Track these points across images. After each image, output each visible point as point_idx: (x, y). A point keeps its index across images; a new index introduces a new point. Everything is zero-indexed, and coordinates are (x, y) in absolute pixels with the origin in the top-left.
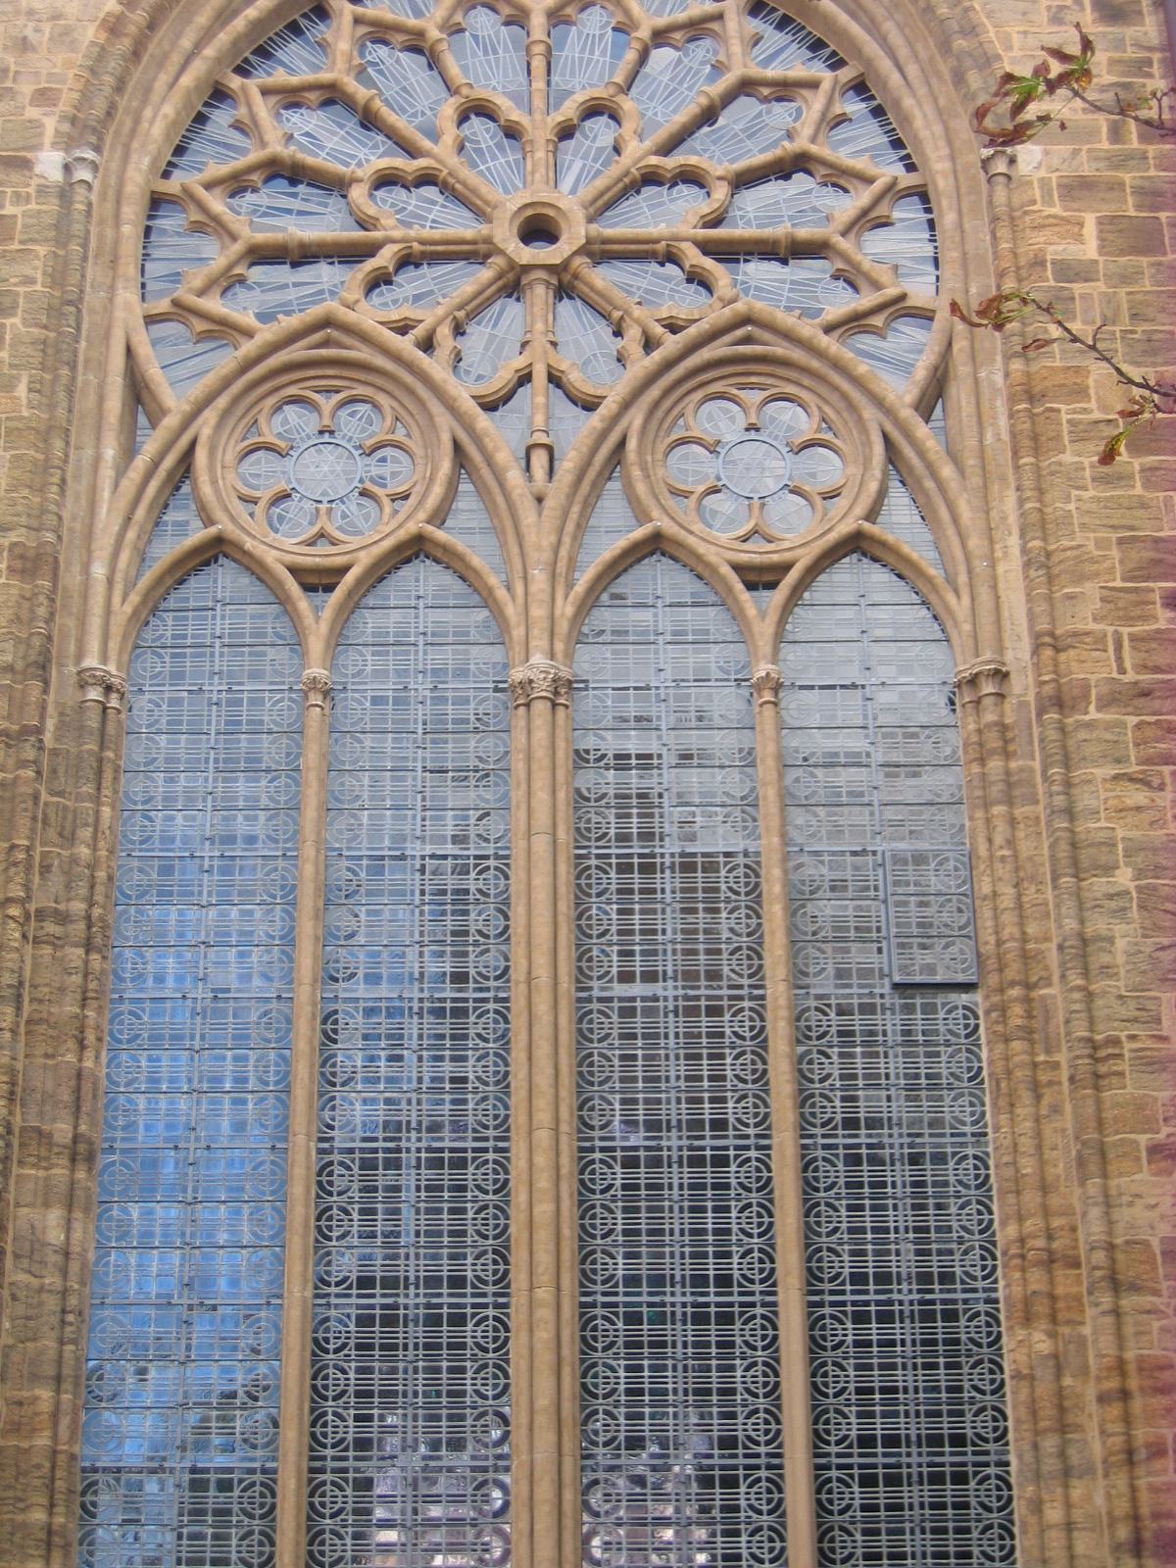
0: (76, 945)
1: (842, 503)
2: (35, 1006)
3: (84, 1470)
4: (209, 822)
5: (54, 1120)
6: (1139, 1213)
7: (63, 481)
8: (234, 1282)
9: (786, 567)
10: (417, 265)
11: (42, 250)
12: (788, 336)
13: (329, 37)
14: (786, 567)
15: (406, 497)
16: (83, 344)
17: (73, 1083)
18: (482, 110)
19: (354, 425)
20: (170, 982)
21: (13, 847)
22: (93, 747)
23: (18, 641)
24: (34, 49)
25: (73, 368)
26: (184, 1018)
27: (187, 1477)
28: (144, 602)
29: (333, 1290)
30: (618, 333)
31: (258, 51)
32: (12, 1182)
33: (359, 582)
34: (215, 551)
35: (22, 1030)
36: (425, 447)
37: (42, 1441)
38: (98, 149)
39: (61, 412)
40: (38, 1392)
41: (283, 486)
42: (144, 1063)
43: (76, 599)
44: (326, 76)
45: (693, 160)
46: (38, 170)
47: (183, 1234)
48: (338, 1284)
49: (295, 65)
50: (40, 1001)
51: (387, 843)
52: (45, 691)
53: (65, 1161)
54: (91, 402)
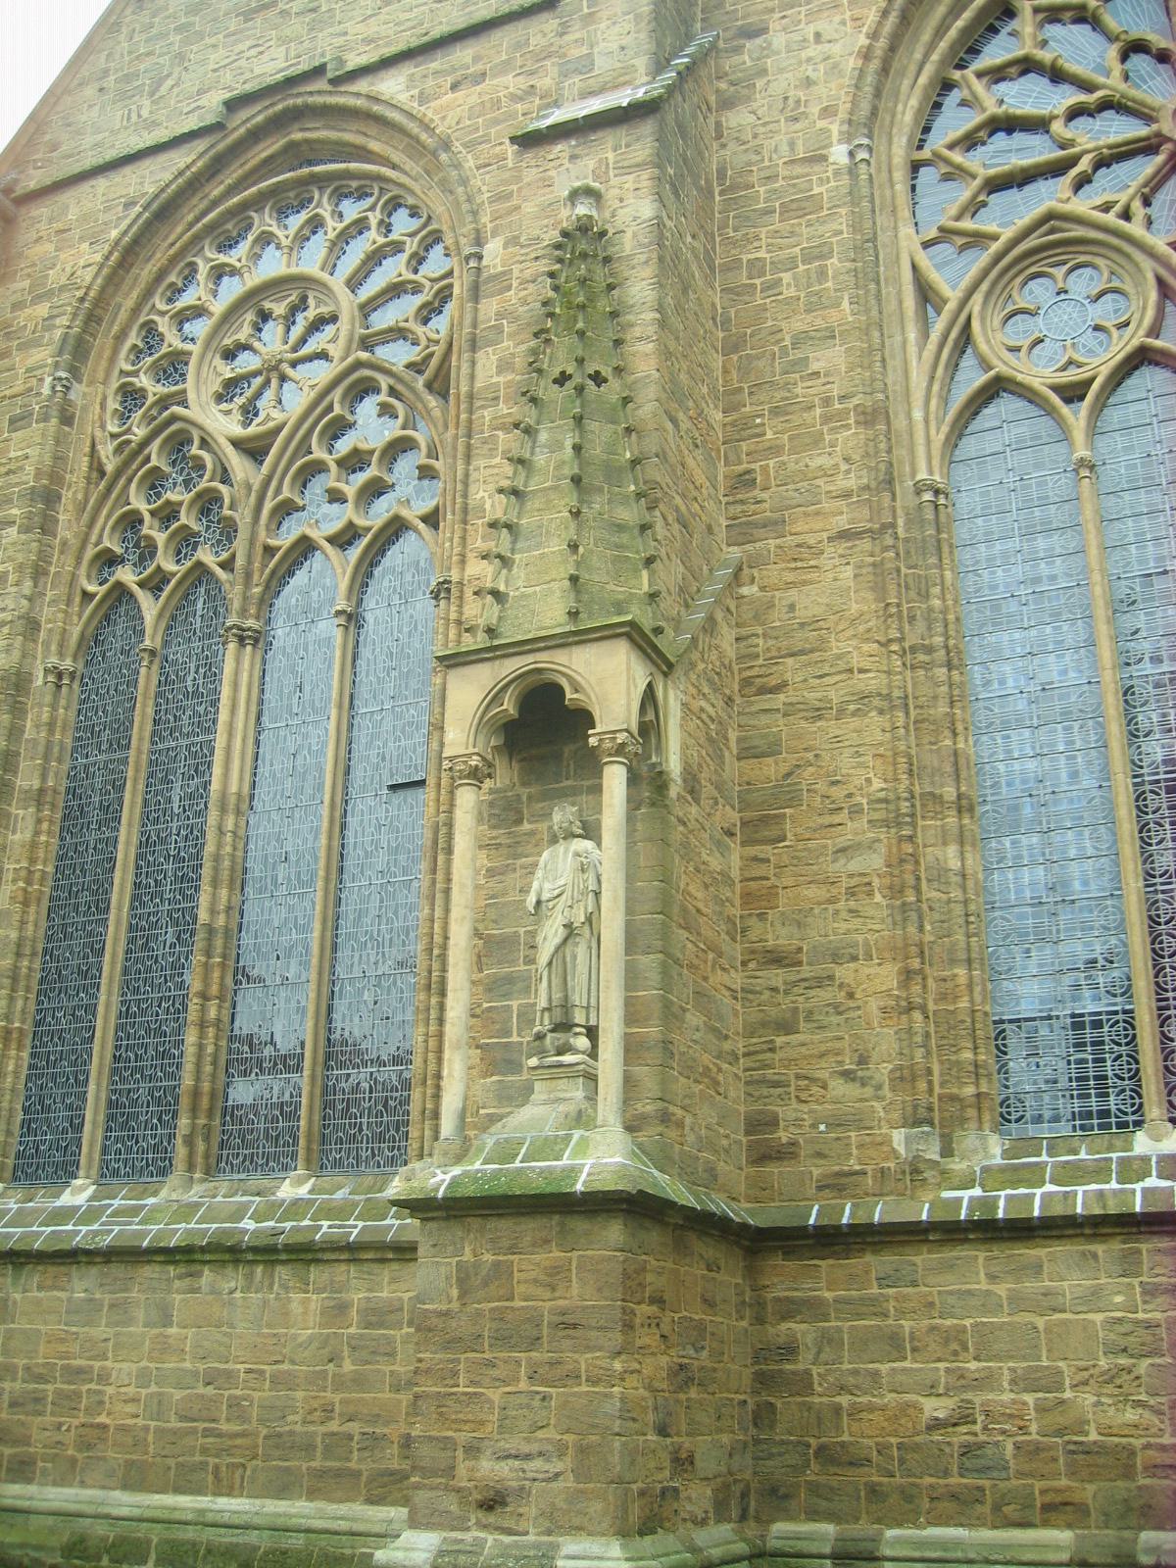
0: (941, 666)
2: (918, 711)
3: (995, 1022)
4: (1019, 571)
5: (942, 786)
7: (883, 360)
8: (1085, 883)
10: (1108, 166)
11: (843, 211)
15: (1128, 324)
16: (882, 269)
17: (952, 759)
19: (1082, 284)
20: (1010, 683)
21: (888, 605)
22: (931, 532)
23: (870, 468)
24: (815, 83)
25: (878, 283)
26: (1021, 705)
27: (1069, 1021)
28: (951, 431)
29: (1158, 880)
31: (969, 48)
32: (919, 829)
33: (1103, 387)
34: (997, 388)
35: (912, 727)
36: (1136, 286)
37: (964, 1004)
38: (870, 137)
39: (874, 313)
40: (956, 971)
41: (1037, 334)
42: (999, 741)
43: (905, 436)
44: (1020, 53)
46: (831, 160)
47: (1044, 854)
48: (1161, 876)
49: (996, 53)
50: (921, 707)
51: (1152, 564)
52: (894, 499)
53: (954, 813)
54: (893, 305)
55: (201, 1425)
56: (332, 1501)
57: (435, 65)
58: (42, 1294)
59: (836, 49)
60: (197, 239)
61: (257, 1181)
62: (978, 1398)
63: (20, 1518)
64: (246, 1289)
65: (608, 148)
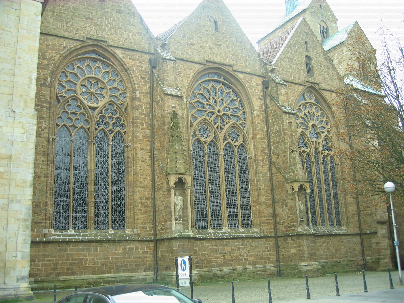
1: (240, 140)
9: (237, 146)
12: (237, 125)
14: (237, 146)
18: (213, 98)
56: (125, 273)
59: (185, 84)
60: (75, 59)
61: (105, 230)
62: (198, 256)
63: (77, 281)
64: (110, 245)
65: (176, 100)
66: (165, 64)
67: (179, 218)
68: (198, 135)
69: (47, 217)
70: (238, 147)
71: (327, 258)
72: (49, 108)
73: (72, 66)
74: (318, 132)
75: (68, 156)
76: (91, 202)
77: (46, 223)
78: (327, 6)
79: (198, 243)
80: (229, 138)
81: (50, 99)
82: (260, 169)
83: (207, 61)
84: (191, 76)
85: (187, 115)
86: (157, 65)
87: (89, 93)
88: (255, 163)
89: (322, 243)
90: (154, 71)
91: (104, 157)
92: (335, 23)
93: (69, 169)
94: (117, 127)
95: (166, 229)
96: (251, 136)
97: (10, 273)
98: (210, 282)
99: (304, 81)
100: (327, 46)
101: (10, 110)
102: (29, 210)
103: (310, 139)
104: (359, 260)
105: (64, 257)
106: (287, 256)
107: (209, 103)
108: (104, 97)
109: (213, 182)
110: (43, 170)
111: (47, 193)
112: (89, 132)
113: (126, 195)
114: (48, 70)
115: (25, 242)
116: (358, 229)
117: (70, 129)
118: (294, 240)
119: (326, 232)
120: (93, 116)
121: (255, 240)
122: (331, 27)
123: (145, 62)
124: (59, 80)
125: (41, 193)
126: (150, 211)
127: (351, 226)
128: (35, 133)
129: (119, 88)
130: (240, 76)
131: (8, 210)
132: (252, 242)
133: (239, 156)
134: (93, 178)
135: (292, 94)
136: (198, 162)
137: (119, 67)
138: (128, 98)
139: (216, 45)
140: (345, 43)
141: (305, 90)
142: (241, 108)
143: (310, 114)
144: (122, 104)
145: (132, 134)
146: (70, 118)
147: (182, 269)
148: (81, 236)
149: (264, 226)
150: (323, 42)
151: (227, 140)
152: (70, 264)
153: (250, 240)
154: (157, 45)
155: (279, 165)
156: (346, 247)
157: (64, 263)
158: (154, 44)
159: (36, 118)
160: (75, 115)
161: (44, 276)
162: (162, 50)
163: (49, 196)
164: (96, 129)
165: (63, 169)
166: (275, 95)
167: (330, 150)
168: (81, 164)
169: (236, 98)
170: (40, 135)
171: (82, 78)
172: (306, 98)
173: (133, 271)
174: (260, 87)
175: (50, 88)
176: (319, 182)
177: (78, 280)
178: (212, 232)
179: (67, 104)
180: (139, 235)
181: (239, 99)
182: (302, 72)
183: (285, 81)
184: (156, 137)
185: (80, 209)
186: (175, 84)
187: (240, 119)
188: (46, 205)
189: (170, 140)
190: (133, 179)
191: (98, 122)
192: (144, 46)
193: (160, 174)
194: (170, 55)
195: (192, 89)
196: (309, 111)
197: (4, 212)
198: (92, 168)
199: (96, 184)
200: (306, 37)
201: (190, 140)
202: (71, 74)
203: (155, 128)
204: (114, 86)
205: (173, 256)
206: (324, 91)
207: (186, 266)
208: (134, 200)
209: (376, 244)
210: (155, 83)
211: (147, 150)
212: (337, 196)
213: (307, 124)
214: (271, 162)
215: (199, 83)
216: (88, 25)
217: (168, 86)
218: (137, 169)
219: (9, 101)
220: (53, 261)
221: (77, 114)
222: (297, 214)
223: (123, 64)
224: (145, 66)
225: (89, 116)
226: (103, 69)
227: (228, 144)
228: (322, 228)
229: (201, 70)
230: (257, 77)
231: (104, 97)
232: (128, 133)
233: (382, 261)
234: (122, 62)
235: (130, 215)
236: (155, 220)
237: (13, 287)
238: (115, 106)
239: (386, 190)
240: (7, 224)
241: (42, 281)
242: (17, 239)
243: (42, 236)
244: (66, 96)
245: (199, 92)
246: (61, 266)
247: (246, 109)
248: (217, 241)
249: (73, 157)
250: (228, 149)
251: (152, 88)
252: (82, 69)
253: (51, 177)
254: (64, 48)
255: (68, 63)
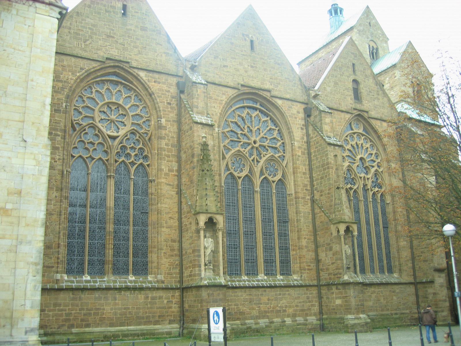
1: (278, 175)
6: (303, 243)
13: (235, 115)
18: (248, 127)
30: (261, 154)
44: (236, 121)
45: (266, 136)
55: (124, 316)
56: (148, 325)
57: (151, 75)
58: (89, 296)
59: (217, 110)
60: (94, 82)
61: (125, 276)
62: (230, 307)
63: (92, 334)
64: (131, 294)
65: (207, 129)
66: (195, 89)
67: (209, 263)
68: (231, 169)
69: (59, 261)
70: (277, 183)
71: (377, 310)
72: (63, 137)
73: (90, 90)
74: (367, 167)
75: (84, 191)
76: (109, 244)
77: (58, 267)
78: (377, 23)
79: (230, 292)
80: (266, 172)
81: (65, 127)
82: (302, 208)
83: (242, 86)
84: (224, 102)
85: (219, 146)
86: (186, 89)
87: (109, 120)
88: (296, 201)
89: (371, 294)
90: (182, 96)
91: (125, 193)
92: (386, 42)
93: (85, 206)
94: (140, 159)
95: (195, 275)
96: (291, 170)
97: (17, 325)
98: (244, 337)
99: (351, 108)
100: (377, 69)
101: (21, 139)
102: (40, 253)
103: (358, 175)
104: (414, 313)
105: (77, 306)
106: (332, 308)
107: (244, 133)
108: (125, 125)
109: (248, 222)
110: (56, 206)
111: (59, 233)
112: (108, 164)
113: (148, 236)
114: (63, 94)
115: (35, 289)
116: (413, 277)
117: (87, 160)
118: (339, 290)
119: (376, 281)
120: (113, 146)
121: (296, 289)
122: (381, 47)
123: (172, 86)
124: (75, 106)
125: (53, 233)
126: (176, 255)
127: (404, 274)
128: (48, 165)
129: (143, 115)
130: (279, 102)
131: (16, 252)
132: (291, 291)
133: (278, 193)
134: (112, 216)
135: (338, 124)
136: (231, 200)
137: (142, 91)
138: (152, 126)
139: (252, 67)
140: (397, 66)
141: (352, 118)
142: (279, 139)
143: (357, 145)
144: (145, 133)
145: (156, 167)
146: (87, 149)
147: (214, 321)
148: (97, 283)
149: (305, 273)
150: (372, 64)
151: (263, 174)
152: (84, 315)
153: (290, 289)
154: (186, 67)
155: (323, 203)
156: (398, 298)
157: (78, 313)
158: (182, 66)
159: (50, 149)
160: (93, 146)
161: (55, 328)
162: (192, 73)
163: (62, 237)
164: (116, 161)
165: (78, 206)
166: (319, 125)
167: (381, 187)
168: (99, 201)
169: (274, 127)
170: (52, 167)
171: (101, 104)
172: (354, 128)
173: (156, 323)
174: (302, 115)
175: (65, 115)
176: (368, 223)
177: (93, 332)
178: (247, 280)
179: (84, 132)
180: (163, 282)
181: (277, 129)
182: (349, 98)
183: (330, 108)
184: (183, 171)
185: (96, 252)
186: (205, 111)
187: (279, 151)
188: (59, 247)
189: (199, 174)
190: (158, 218)
191: (118, 153)
192: (172, 68)
193: (188, 213)
194: (200, 78)
195: (224, 116)
196: (356, 143)
197: (13, 254)
198: (111, 206)
199: (115, 224)
200: (354, 59)
201: (222, 175)
202: (88, 99)
203: (183, 160)
204: (137, 112)
205: (201, 306)
206: (374, 120)
207: (219, 318)
208: (158, 242)
209: (432, 295)
210: (183, 110)
211: (173, 185)
212: (389, 239)
213: (354, 157)
214: (313, 201)
215: (232, 109)
216: (108, 44)
217: (198, 113)
218: (162, 207)
219: (20, 129)
220: (66, 310)
221: (95, 143)
222: (342, 260)
223: (147, 87)
224: (172, 91)
225: (109, 147)
226: (125, 94)
227: (265, 180)
228: (372, 276)
229: (235, 95)
230: (298, 104)
231: (125, 125)
232: (152, 166)
233: (440, 314)
234: (146, 86)
235: (153, 259)
236: (181, 265)
237: (20, 340)
238: (138, 135)
239: (445, 233)
240: (15, 268)
241: (52, 334)
242: (26, 285)
243: (53, 282)
244: (82, 123)
245: (233, 120)
246: (75, 316)
247: (285, 140)
248: (251, 289)
249: (89, 193)
250: (265, 185)
251: (179, 115)
252: (101, 93)
253: (65, 215)
254: (82, 69)
255: (85, 86)
